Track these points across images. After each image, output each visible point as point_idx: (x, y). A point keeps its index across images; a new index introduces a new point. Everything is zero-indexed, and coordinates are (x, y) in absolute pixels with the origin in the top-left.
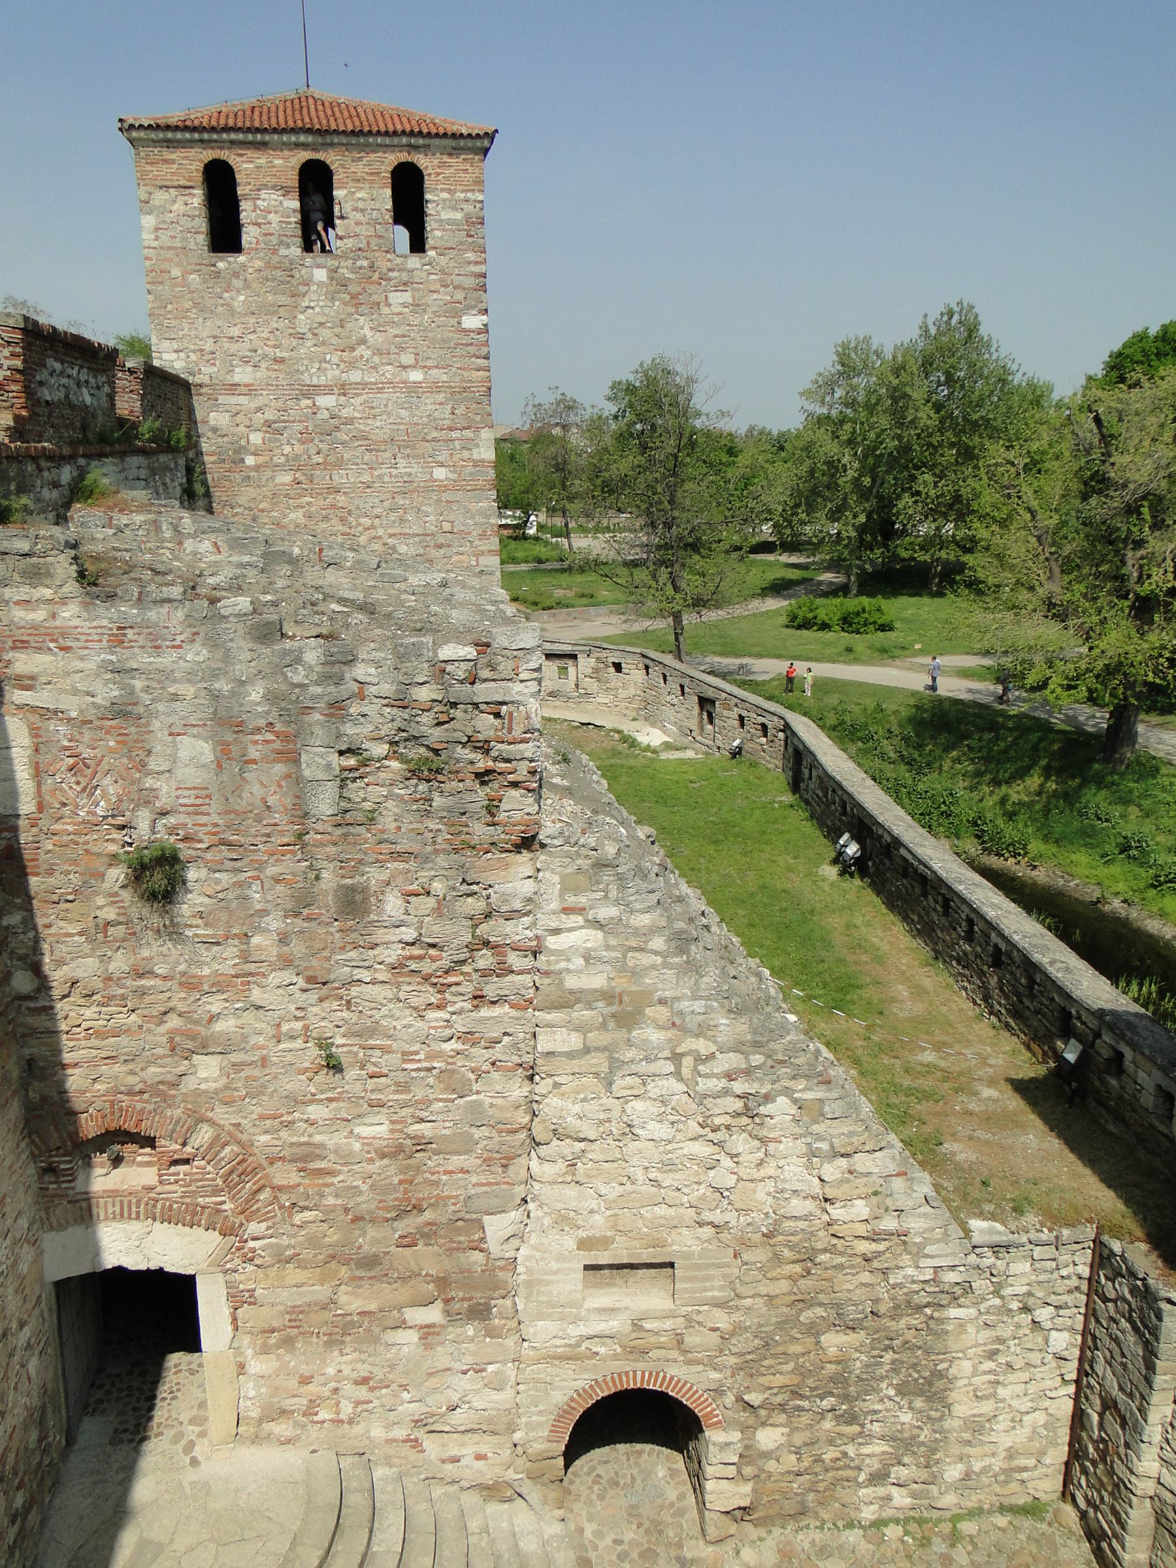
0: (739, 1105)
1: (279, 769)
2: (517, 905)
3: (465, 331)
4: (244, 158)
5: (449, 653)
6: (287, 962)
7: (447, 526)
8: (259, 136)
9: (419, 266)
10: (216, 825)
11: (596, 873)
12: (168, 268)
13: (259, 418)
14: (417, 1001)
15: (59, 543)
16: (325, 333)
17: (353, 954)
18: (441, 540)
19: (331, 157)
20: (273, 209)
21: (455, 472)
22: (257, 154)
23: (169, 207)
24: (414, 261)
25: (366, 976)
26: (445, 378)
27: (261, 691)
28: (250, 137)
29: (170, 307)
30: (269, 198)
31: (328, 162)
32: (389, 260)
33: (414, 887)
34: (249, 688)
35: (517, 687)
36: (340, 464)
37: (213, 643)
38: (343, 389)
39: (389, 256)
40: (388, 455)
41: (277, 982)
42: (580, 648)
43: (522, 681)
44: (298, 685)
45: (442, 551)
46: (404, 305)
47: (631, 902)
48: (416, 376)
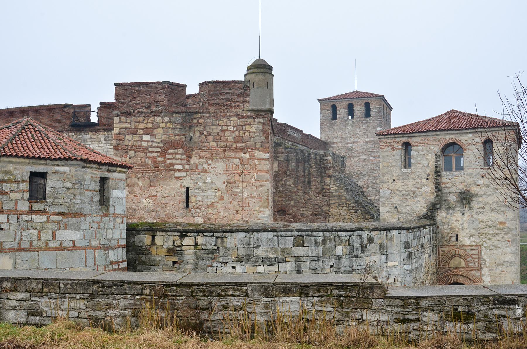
0: (354, 211)
7: (373, 168)
13: (338, 148)
18: (371, 171)
19: (353, 102)
24: (368, 119)
25: (310, 192)
36: (352, 156)
38: (354, 142)
48: (367, 140)
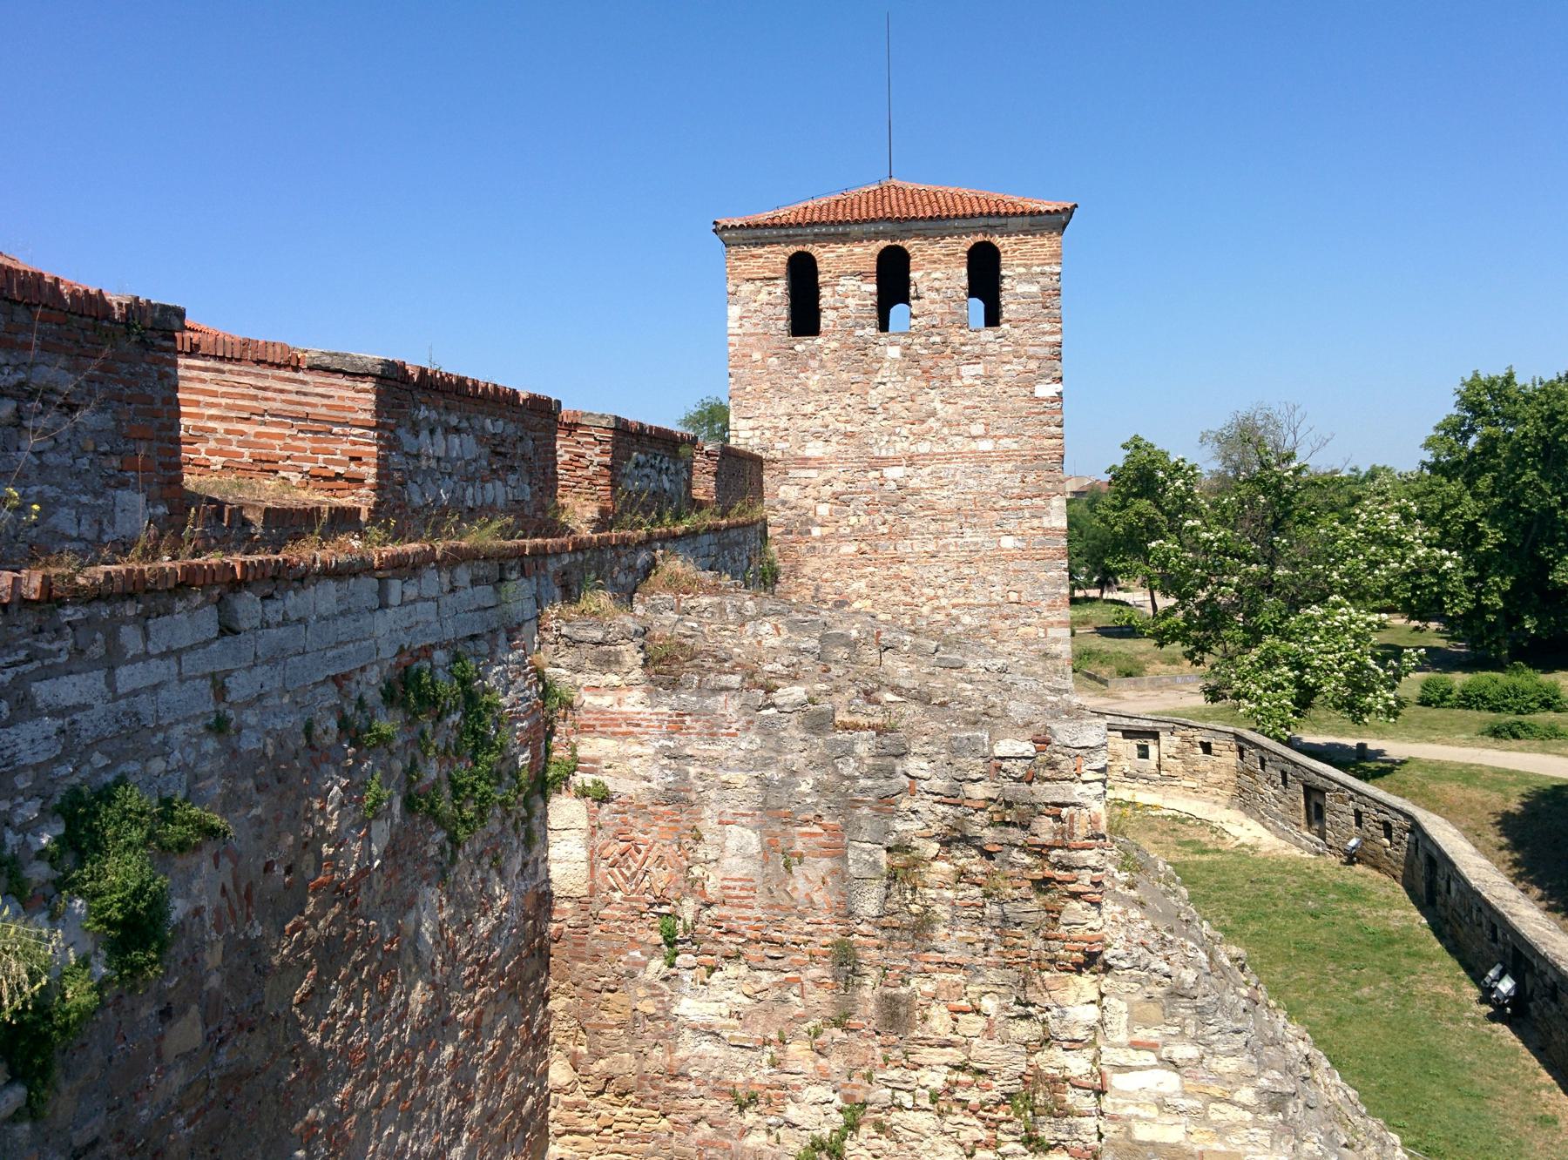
1: (826, 863)
2: (1079, 1035)
3: (1037, 399)
5: (1007, 749)
6: (824, 1078)
7: (1013, 597)
10: (759, 920)
11: (1170, 1004)
14: (965, 1136)
15: (630, 632)
16: (896, 407)
17: (895, 1074)
18: (1006, 611)
19: (910, 245)
21: (1023, 540)
24: (988, 334)
26: (1015, 446)
27: (811, 782)
29: (749, 389)
30: (848, 284)
32: (962, 335)
33: (963, 1003)
34: (800, 779)
35: (1080, 788)
37: (767, 729)
38: (911, 461)
39: (962, 331)
40: (954, 524)
41: (811, 1098)
42: (1163, 725)
43: (1084, 782)
44: (848, 778)
45: (1008, 622)
46: (976, 377)
47: (1213, 1042)
48: (986, 445)
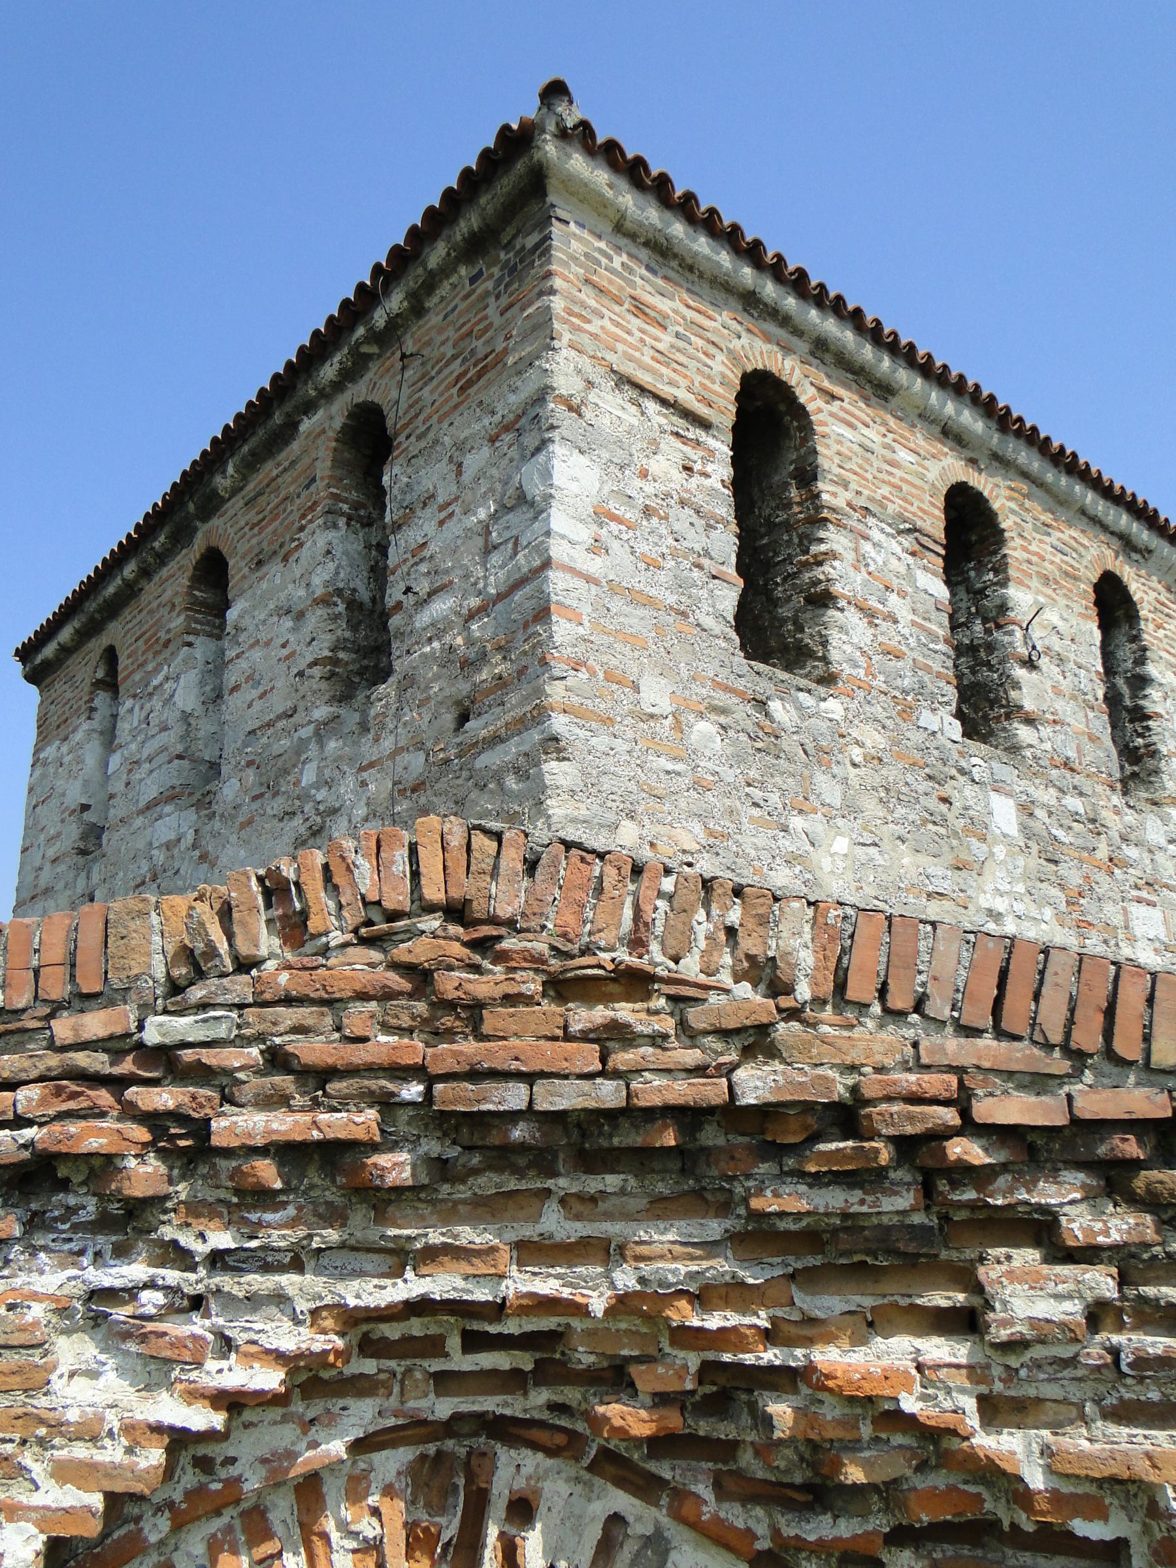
4: (835, 406)
8: (886, 363)
9: (1163, 842)
12: (633, 671)
20: (895, 583)
22: (861, 410)
23: (640, 460)
28: (867, 352)
31: (996, 505)
